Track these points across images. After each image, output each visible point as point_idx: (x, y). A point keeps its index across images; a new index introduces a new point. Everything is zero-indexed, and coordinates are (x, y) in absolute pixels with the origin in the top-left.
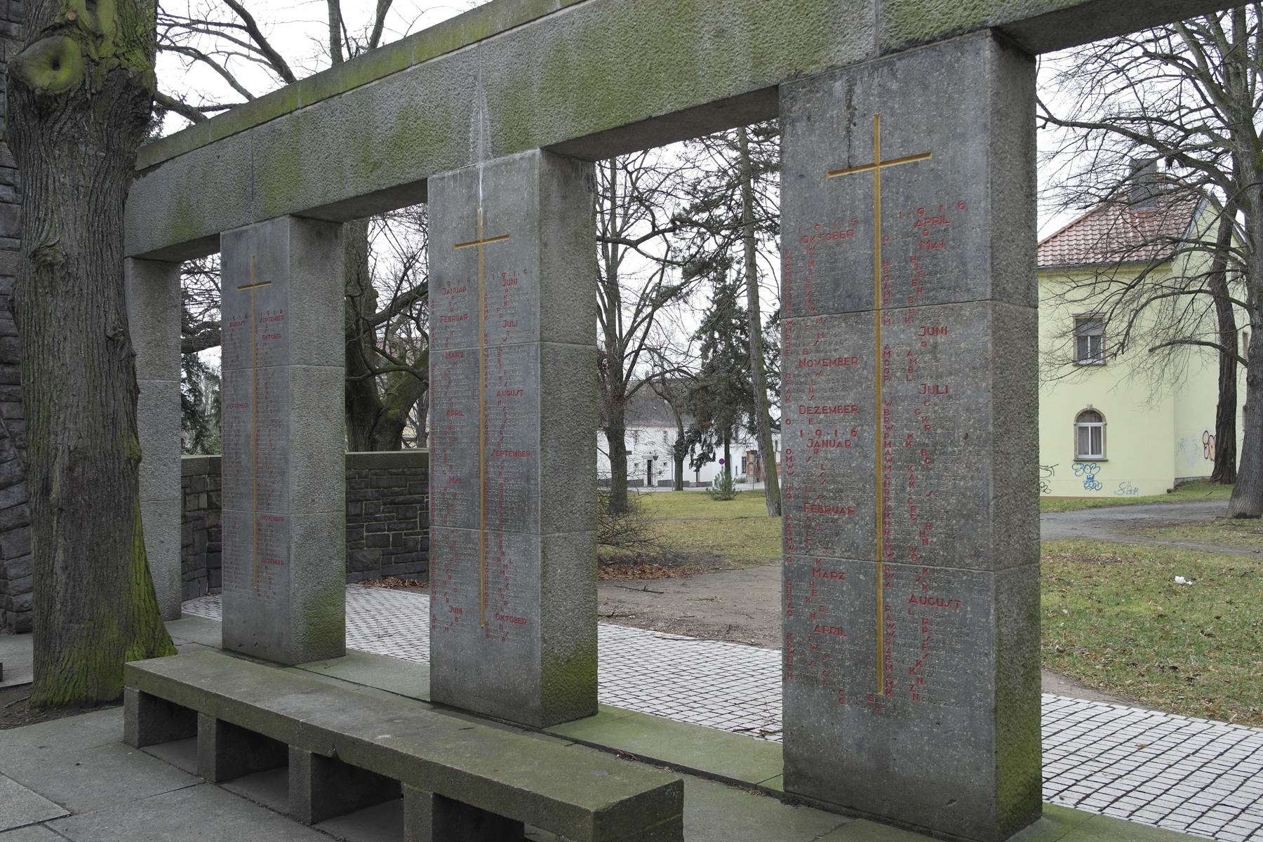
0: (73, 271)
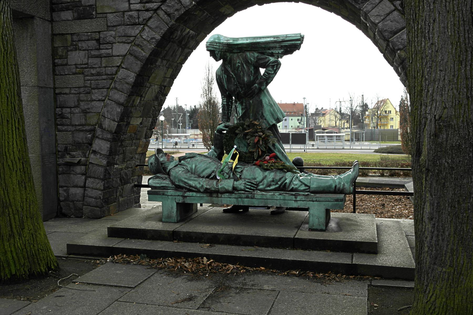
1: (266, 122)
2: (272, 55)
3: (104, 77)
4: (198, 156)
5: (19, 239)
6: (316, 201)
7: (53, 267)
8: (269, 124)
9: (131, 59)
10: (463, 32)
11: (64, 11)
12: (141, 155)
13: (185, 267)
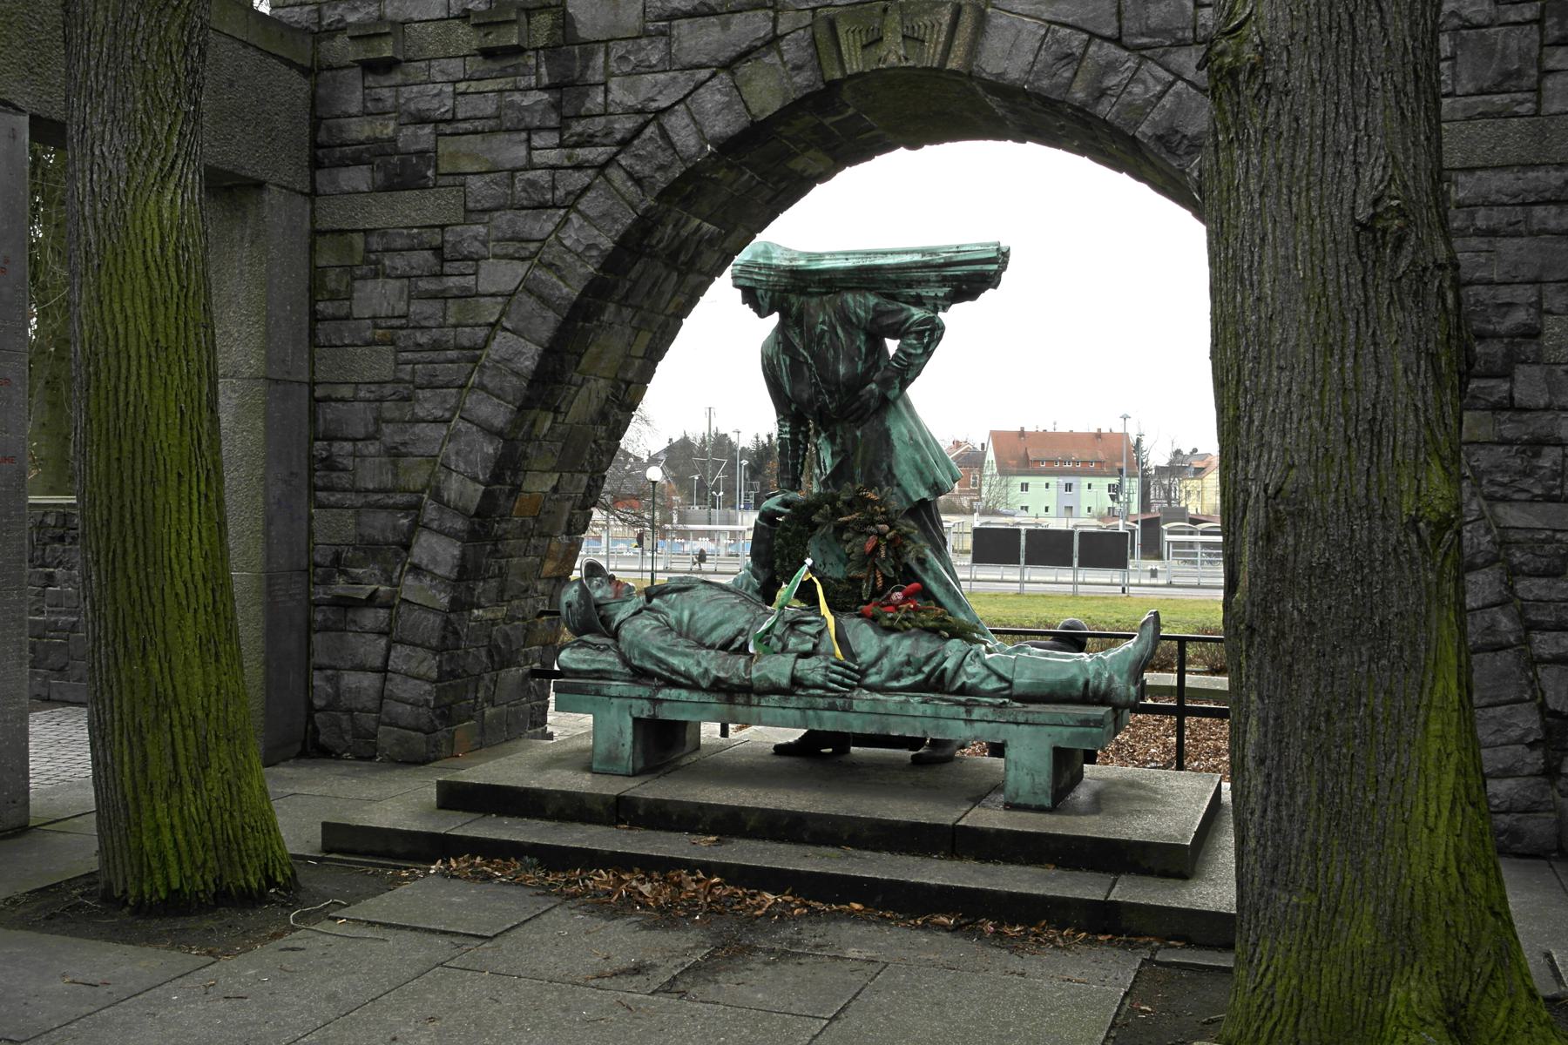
0: (1276, 79)
1: (900, 494)
2: (919, 301)
3: (452, 354)
4: (701, 586)
5: (194, 793)
6: (1026, 723)
7: (279, 879)
8: (909, 499)
9: (530, 303)
10: (1333, 271)
11: (348, 166)
12: (553, 582)
13: (641, 894)
